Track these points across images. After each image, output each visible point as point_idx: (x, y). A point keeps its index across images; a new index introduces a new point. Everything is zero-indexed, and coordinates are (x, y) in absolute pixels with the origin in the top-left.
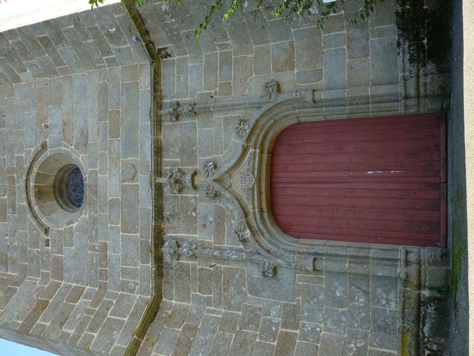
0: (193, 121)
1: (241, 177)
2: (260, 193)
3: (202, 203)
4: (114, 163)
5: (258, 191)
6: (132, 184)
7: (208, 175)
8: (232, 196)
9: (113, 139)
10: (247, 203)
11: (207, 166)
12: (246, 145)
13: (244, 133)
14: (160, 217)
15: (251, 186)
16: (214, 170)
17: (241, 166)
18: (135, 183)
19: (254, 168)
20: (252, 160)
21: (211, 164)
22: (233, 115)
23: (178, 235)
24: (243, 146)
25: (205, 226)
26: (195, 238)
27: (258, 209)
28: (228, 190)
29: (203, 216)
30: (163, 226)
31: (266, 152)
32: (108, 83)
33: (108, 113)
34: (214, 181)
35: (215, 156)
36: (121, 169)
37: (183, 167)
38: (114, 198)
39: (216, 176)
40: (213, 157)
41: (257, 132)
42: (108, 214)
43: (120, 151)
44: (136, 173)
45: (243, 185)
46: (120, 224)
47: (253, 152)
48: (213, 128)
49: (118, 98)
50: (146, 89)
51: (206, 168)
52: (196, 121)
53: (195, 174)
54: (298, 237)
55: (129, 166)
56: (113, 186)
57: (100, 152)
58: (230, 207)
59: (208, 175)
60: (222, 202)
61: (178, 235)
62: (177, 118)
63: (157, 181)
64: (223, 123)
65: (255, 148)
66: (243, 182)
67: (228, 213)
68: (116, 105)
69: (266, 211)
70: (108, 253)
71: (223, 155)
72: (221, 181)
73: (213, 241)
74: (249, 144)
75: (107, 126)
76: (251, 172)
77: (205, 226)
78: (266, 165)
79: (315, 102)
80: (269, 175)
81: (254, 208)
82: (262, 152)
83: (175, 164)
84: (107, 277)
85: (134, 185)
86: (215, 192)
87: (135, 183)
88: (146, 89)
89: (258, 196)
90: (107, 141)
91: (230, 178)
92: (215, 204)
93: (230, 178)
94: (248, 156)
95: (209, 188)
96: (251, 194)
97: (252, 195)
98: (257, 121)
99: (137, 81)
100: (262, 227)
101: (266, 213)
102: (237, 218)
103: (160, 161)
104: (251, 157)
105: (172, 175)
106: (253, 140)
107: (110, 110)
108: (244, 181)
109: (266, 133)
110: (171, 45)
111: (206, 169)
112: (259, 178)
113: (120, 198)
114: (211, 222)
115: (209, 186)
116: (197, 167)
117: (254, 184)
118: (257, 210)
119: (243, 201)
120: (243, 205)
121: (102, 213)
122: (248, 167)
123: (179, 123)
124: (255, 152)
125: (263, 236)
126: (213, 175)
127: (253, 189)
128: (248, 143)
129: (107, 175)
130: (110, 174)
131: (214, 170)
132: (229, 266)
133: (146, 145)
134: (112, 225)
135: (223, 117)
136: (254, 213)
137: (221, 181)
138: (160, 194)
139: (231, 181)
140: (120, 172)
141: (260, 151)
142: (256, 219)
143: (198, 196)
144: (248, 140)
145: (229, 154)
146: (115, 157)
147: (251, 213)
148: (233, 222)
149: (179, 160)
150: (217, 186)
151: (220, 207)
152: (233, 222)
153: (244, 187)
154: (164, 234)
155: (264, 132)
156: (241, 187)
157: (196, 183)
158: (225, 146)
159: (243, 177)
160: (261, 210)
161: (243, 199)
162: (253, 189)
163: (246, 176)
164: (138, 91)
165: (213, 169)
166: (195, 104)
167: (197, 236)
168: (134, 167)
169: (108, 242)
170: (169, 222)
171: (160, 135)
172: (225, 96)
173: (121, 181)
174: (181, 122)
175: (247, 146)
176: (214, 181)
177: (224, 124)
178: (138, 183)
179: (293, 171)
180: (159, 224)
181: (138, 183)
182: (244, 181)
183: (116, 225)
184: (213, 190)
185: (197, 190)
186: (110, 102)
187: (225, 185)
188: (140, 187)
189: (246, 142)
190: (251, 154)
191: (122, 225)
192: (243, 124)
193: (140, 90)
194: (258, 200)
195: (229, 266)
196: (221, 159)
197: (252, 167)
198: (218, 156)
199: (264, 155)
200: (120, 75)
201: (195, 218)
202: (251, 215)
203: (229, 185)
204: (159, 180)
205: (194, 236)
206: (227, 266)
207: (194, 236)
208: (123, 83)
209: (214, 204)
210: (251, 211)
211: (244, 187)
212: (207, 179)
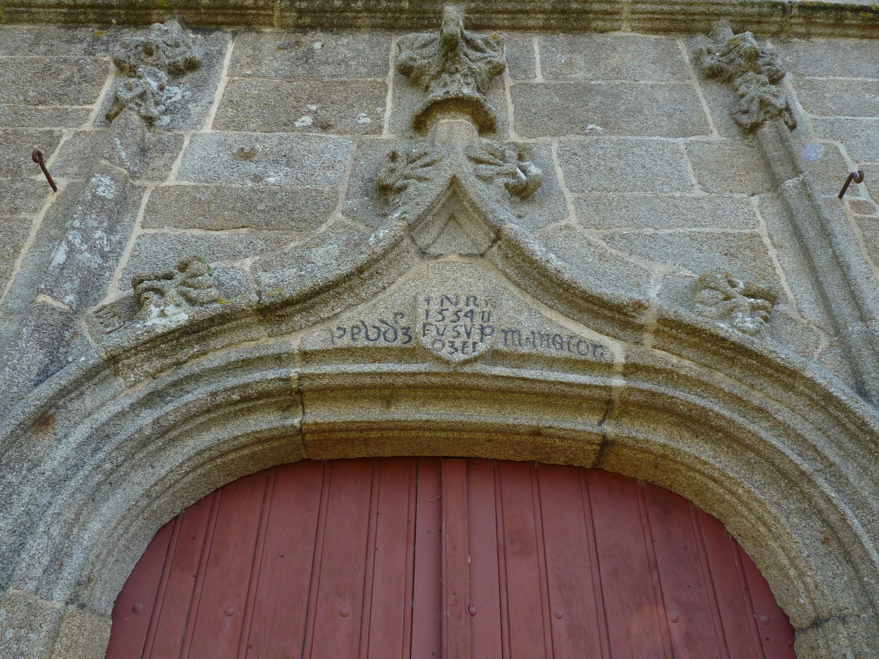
0: (712, 127)
1: (472, 299)
3: (354, 148)
5: (400, 381)
7: (478, 161)
8: (379, 251)
10: (336, 323)
11: (521, 158)
12: (648, 318)
13: (714, 309)
14: (307, 20)
15: (426, 341)
16: (507, 186)
17: (529, 299)
19: (524, 359)
20: (565, 354)
21: (534, 170)
22: (779, 271)
23: (225, 72)
24: (639, 306)
25: (247, 156)
26: (199, 123)
27: (301, 377)
28: (407, 241)
29: (291, 149)
30: (268, 30)
31: (610, 429)
34: (454, 181)
35: (569, 197)
37: (508, 92)
39: (474, 188)
40: (566, 191)
41: (721, 378)
45: (435, 307)
47: (607, 357)
48: (698, 192)
51: (515, 155)
52: (715, 137)
58: (321, 251)
59: (478, 161)
60: (349, 222)
61: (224, 73)
64: (729, 230)
65: (631, 369)
66: (447, 304)
67: (292, 245)
69: (288, 422)
71: (580, 228)
72: (452, 217)
73: (171, 181)
74: (648, 339)
76: (501, 346)
77: (247, 156)
78: (537, 432)
80: (479, 452)
81: (306, 356)
86: (399, 184)
89: (368, 381)
91: (468, 255)
92: (343, 196)
93: (468, 255)
96: (382, 343)
97: (378, 350)
100: (198, 394)
101: (277, 424)
102: (266, 278)
103: (531, 23)
104: (582, 347)
105: (476, 48)
106: (675, 360)
108: (452, 309)
109: (720, 429)
111: (507, 153)
112: (470, 389)
115: (427, 165)
117: (439, 359)
118: (293, 371)
119: (349, 307)
120: (326, 303)
122: (525, 334)
123: (695, 82)
124: (608, 367)
125: (151, 399)
126: (479, 177)
128: (657, 332)
131: (507, 186)
135: (762, 229)
136: (279, 359)
137: (452, 217)
138: (397, 19)
139: (454, 258)
141: (616, 396)
142: (246, 364)
145: (583, 251)
147: (281, 340)
148: (248, 262)
149: (539, 79)
151: (327, 213)
152: (248, 262)
153: (421, 311)
154: (235, 34)
155: (727, 413)
156: (421, 298)
157: (441, 121)
158: (623, 237)
159: (472, 307)
161: (361, 307)
163: (478, 320)
165: (512, 181)
167: (207, 129)
171: (633, 30)
172: (862, 244)
174: (699, 91)
175: (641, 328)
176: (454, 181)
177: (726, 235)
179: (503, 584)
180: (277, 13)
182: (452, 309)
185: (411, 133)
187: (434, 230)
189: (664, 321)
190: (595, 347)
192: (754, 309)
194: (348, 381)
196: (555, 220)
197: (525, 350)
198: (571, 207)
199: (595, 419)
201: (288, 125)
202: (272, 341)
203: (432, 250)
206: (33, 233)
209: (342, 189)
210: (294, 343)
211: (421, 311)
212: (462, 158)
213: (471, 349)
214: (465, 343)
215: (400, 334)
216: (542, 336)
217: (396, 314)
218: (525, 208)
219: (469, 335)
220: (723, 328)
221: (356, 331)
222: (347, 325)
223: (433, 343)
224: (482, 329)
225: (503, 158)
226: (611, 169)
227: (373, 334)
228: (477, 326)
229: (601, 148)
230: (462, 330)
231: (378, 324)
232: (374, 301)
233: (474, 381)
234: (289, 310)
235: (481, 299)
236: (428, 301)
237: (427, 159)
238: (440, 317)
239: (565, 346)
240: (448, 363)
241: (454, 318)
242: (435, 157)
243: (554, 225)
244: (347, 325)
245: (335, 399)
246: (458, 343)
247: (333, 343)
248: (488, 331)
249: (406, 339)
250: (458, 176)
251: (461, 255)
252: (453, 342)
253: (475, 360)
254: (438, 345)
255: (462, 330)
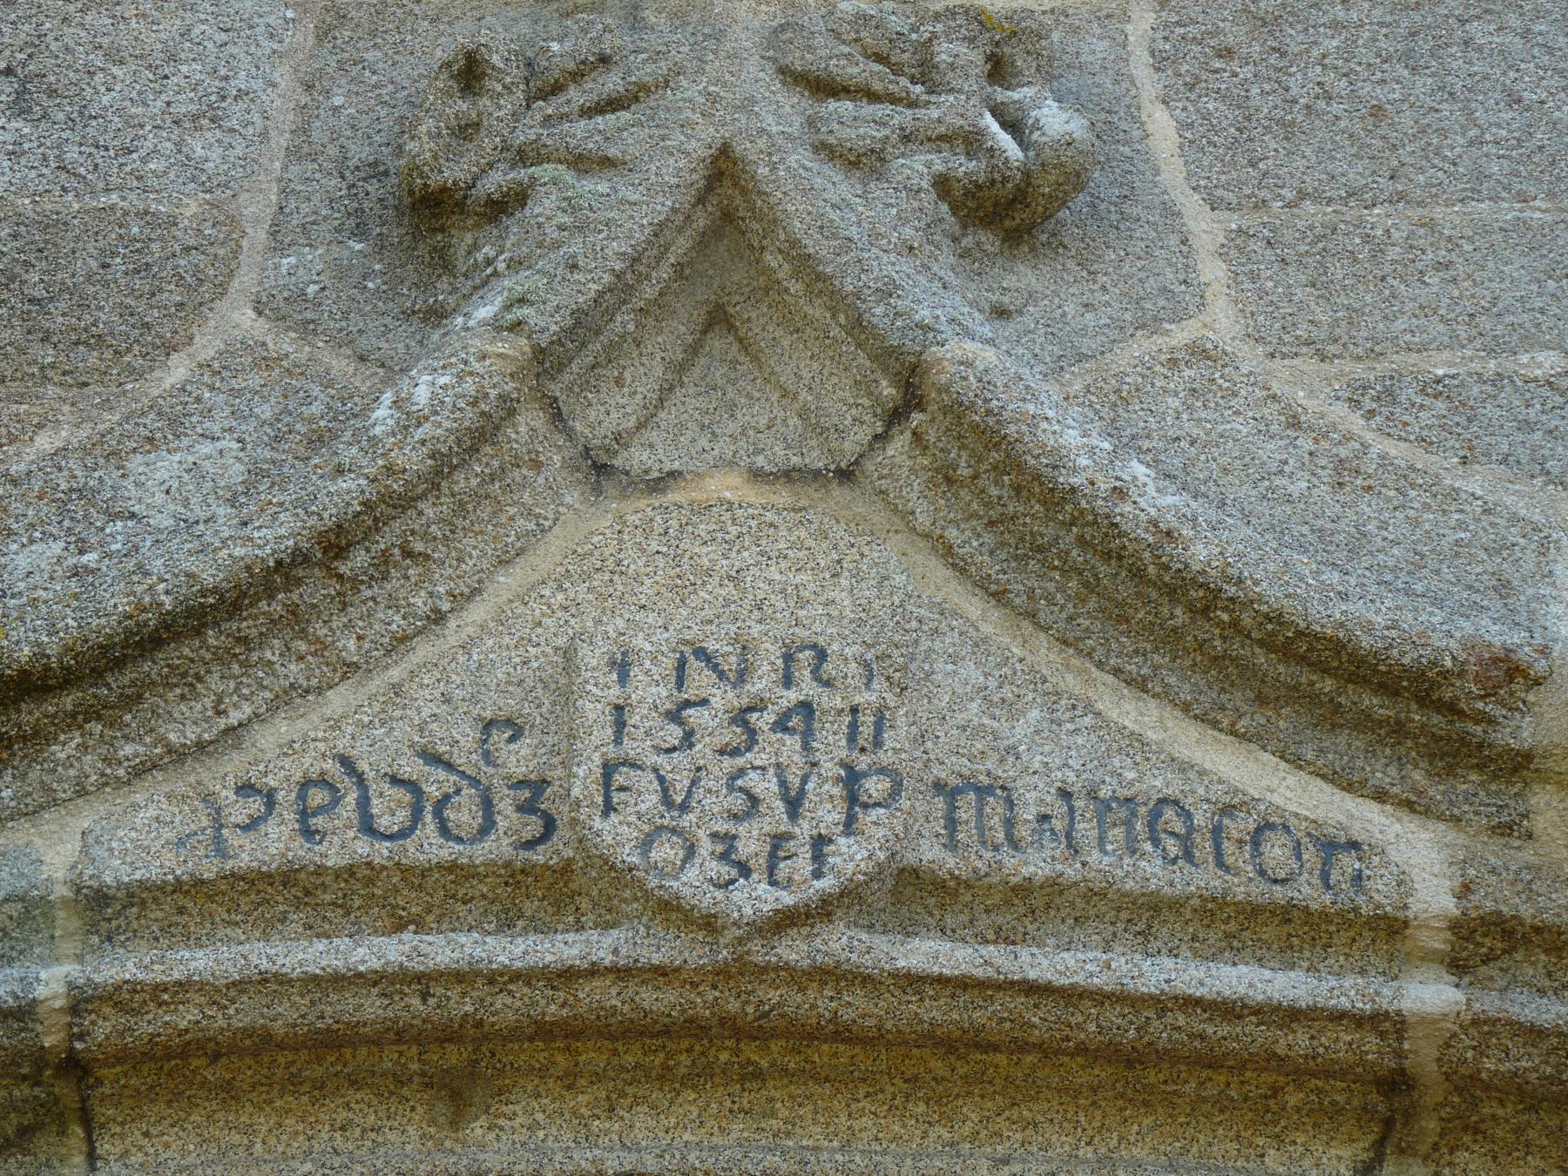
3: (302, 37)
5: (506, 1008)
7: (823, 87)
8: (413, 459)
10: (233, 765)
11: (998, 70)
16: (942, 185)
17: (1044, 654)
20: (1203, 879)
27: (81, 1002)
28: (530, 420)
29: (35, 45)
40: (1192, 206)
47: (1381, 890)
51: (974, 58)
58: (167, 466)
59: (823, 87)
60: (285, 344)
66: (701, 680)
67: (45, 442)
71: (1251, 358)
72: (718, 319)
76: (930, 853)
86: (495, 182)
89: (372, 1008)
91: (788, 475)
92: (258, 236)
93: (788, 475)
95: (576, 96)
96: (429, 846)
97: (414, 876)
104: (1276, 852)
108: (723, 698)
111: (944, 52)
112: (804, 1035)
115: (612, 105)
117: (670, 910)
119: (287, 698)
120: (187, 681)
122: (1033, 799)
126: (827, 151)
131: (942, 185)
137: (718, 319)
139: (727, 486)
141: (1423, 1056)
145: (1270, 451)
151: (192, 309)
153: (594, 711)
156: (592, 657)
158: (1435, 388)
159: (807, 688)
161: (338, 700)
163: (832, 743)
165: (964, 166)
182: (723, 698)
184: (523, 157)
187: (645, 374)
190: (1332, 846)
194: (285, 1014)
196: (1150, 325)
197: (1036, 864)
198: (1212, 271)
203: (637, 458)
209: (257, 207)
211: (594, 711)
212: (757, 77)
213: (803, 864)
214: (778, 840)
215: (505, 807)
216: (1104, 807)
217: (489, 725)
218: (1023, 277)
219: (794, 804)
221: (318, 797)
222: (282, 776)
223: (646, 844)
224: (852, 779)
225: (927, 73)
226: (1377, 112)
227: (389, 810)
228: (830, 768)
229: (1336, 25)
230: (765, 786)
231: (410, 767)
232: (395, 674)
233: (821, 1003)
234: (30, 714)
235: (845, 655)
236: (622, 667)
237: (612, 83)
238: (674, 734)
239: (1202, 850)
240: (710, 924)
241: (734, 735)
242: (645, 72)
243: (1142, 346)
244: (282, 776)
245: (228, 1093)
246: (751, 843)
247: (220, 848)
248: (875, 787)
249: (534, 827)
250: (741, 147)
251: (757, 475)
252: (729, 839)
253: (823, 910)
254: (666, 851)
255: (765, 786)
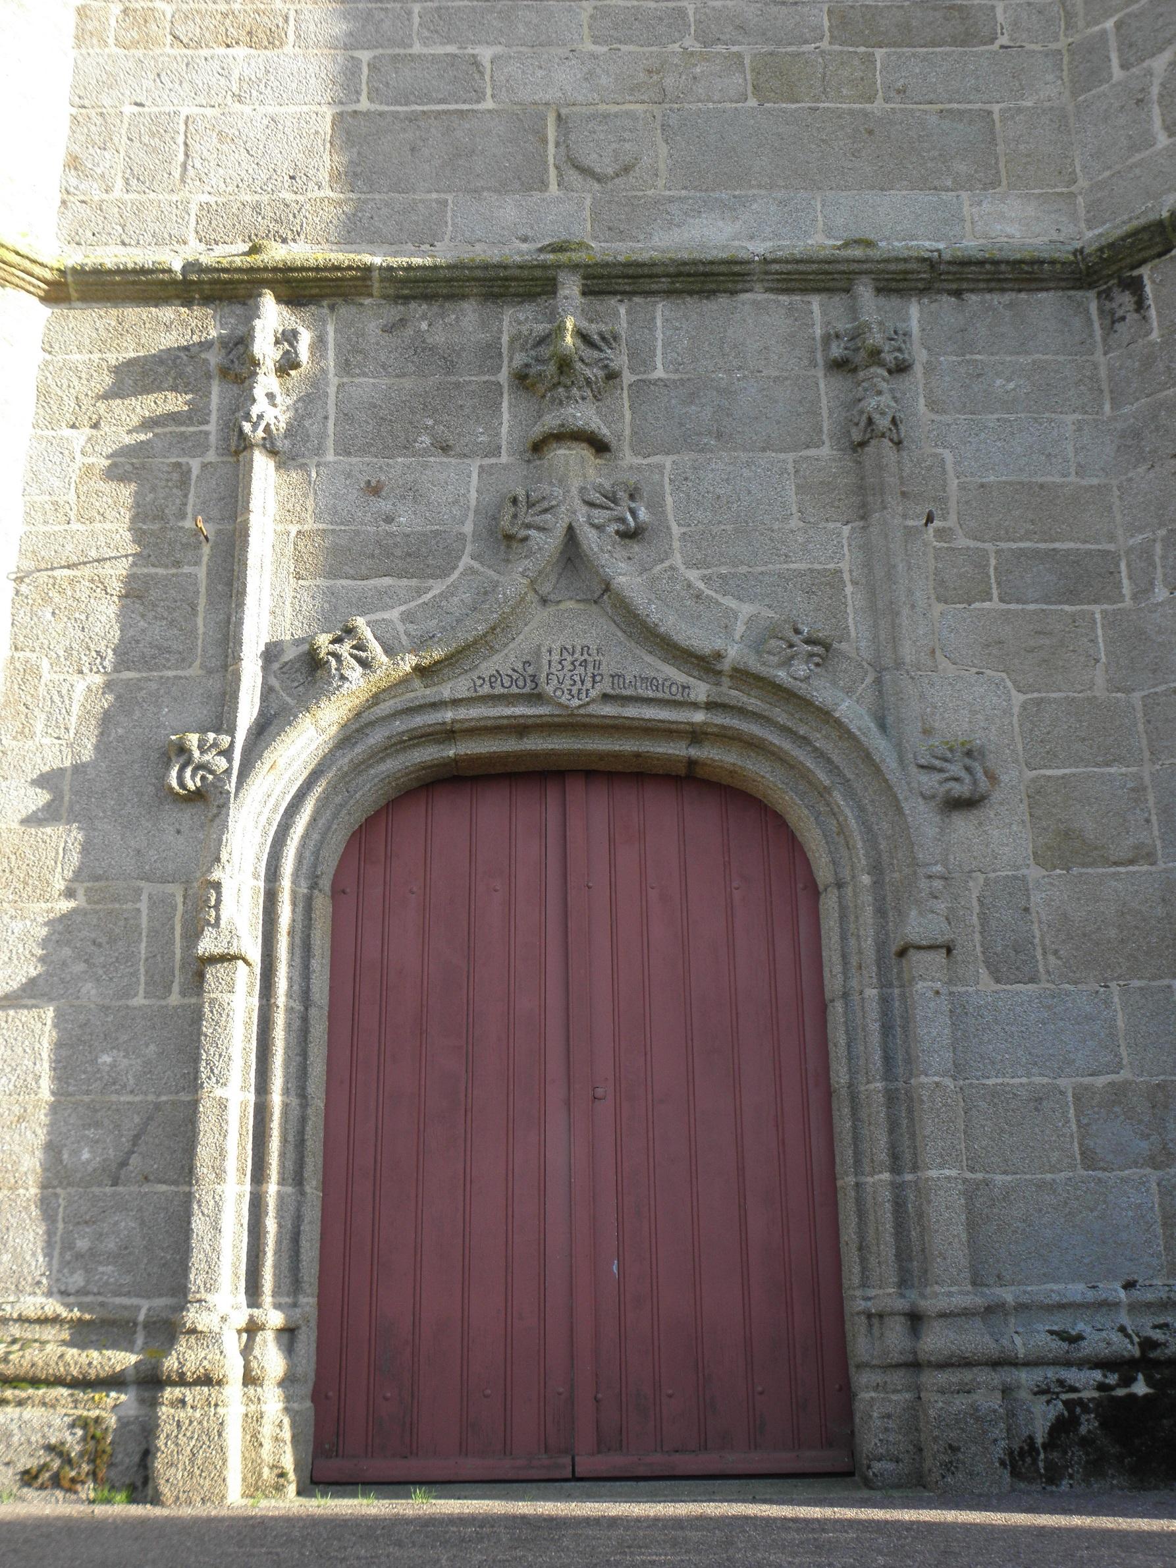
0: (824, 437)
1: (585, 649)
2: (521, 729)
4: (642, 76)
5: (530, 721)
6: (551, 160)
7: (591, 504)
9: (748, 71)
12: (726, 665)
13: (776, 659)
15: (549, 689)
16: (617, 532)
18: (552, 172)
21: (643, 514)
22: (850, 610)
24: (719, 656)
25: (374, 490)
30: (367, 301)
31: (694, 752)
32: (995, 46)
33: (862, 49)
34: (571, 533)
35: (676, 530)
36: (614, 109)
37: (625, 392)
38: (487, 78)
39: (590, 538)
41: (780, 715)
42: (417, 48)
43: (693, 107)
44: (599, 181)
45: (556, 657)
46: (374, 107)
47: (693, 697)
48: (794, 523)
49: (932, 96)
50: (968, 225)
52: (826, 451)
53: (600, 446)
54: (337, 892)
55: (627, 146)
56: (540, 73)
57: (691, 13)
59: (591, 504)
62: (840, 366)
63: (562, 276)
64: (817, 566)
65: (710, 706)
66: (565, 654)
68: (899, 84)
69: (445, 754)
70: (240, 51)
71: (682, 568)
74: (726, 681)
75: (806, 42)
76: (609, 691)
77: (374, 490)
78: (638, 755)
79: (902, 953)
80: (594, 767)
81: (455, 703)
82: (696, 735)
83: (641, 358)
84: (135, 44)
85: (546, 170)
87: (552, 172)
88: (968, 225)
89: (505, 722)
90: (741, 44)
94: (680, 677)
95: (538, 508)
96: (514, 690)
98: (825, 716)
99: (1004, 183)
101: (436, 756)
103: (654, 287)
104: (674, 689)
106: (745, 699)
107: (878, 57)
108: (570, 659)
109: (773, 754)
110: (1155, 336)
113: (489, 104)
114: (389, 520)
115: (546, 511)
116: (628, 458)
117: (560, 705)
121: (416, 20)
122: (628, 678)
123: (820, 373)
126: (593, 525)
127: (536, 697)
128: (731, 677)
129: (589, 47)
130: (594, 56)
131: (617, 532)
132: (202, 601)
133: (720, 223)
134: (365, 70)
135: (845, 566)
136: (435, 706)
140: (602, 107)
143: (504, 459)
144: (742, 676)
146: (669, 81)
147: (435, 689)
150: (548, 544)
153: (545, 662)
154: (332, 308)
155: (776, 742)
156: (544, 650)
157: (560, 452)
158: (720, 576)
159: (586, 656)
160: (449, 734)
161: (495, 658)
162: (536, 697)
164: (958, 186)
165: (622, 527)
166: (898, 443)
168: (627, 169)
169: (288, 49)
170: (388, 329)
171: (767, 290)
172: (932, 577)
173: (564, 111)
175: (720, 673)
176: (571, 533)
177: (811, 571)
178: (553, 187)
179: (612, 865)
181: (553, 187)
182: (570, 659)
183: (364, 87)
184: (528, 526)
185: (528, 455)
186: (914, 55)
188: (537, 195)
189: (735, 670)
191: (366, 114)
192: (811, 655)
193: (964, 195)
194: (489, 723)
195: (202, 601)
196: (662, 561)
197: (628, 692)
198: (676, 544)
199: (683, 744)
200: (1030, 104)
202: (428, 691)
204: (570, 288)
205: (330, 443)
206: (203, 590)
207: (330, 443)
208: (996, 116)
210: (446, 691)
211: (545, 662)
212: (577, 502)
213: (583, 696)
214: (580, 690)
215: (528, 681)
216: (642, 679)
217: (524, 663)
218: (636, 548)
219: (583, 682)
220: (782, 675)
221: (493, 679)
222: (486, 675)
223: (555, 692)
224: (594, 676)
225: (615, 501)
226: (719, 497)
227: (507, 684)
228: (590, 674)
229: (712, 470)
230: (577, 678)
231: (510, 672)
232: (506, 651)
233: (588, 720)
234: (439, 666)
235: (593, 648)
236: (550, 652)
237: (545, 504)
238: (560, 667)
239: (660, 688)
240: (567, 707)
241: (571, 667)
242: (554, 503)
243: (659, 567)
244: (486, 675)
245: (480, 735)
246: (574, 692)
247: (476, 691)
248: (598, 678)
249: (533, 685)
250: (574, 524)
251: (578, 601)
252: (570, 690)
253: (588, 703)
254: (559, 693)
255: (577, 678)
